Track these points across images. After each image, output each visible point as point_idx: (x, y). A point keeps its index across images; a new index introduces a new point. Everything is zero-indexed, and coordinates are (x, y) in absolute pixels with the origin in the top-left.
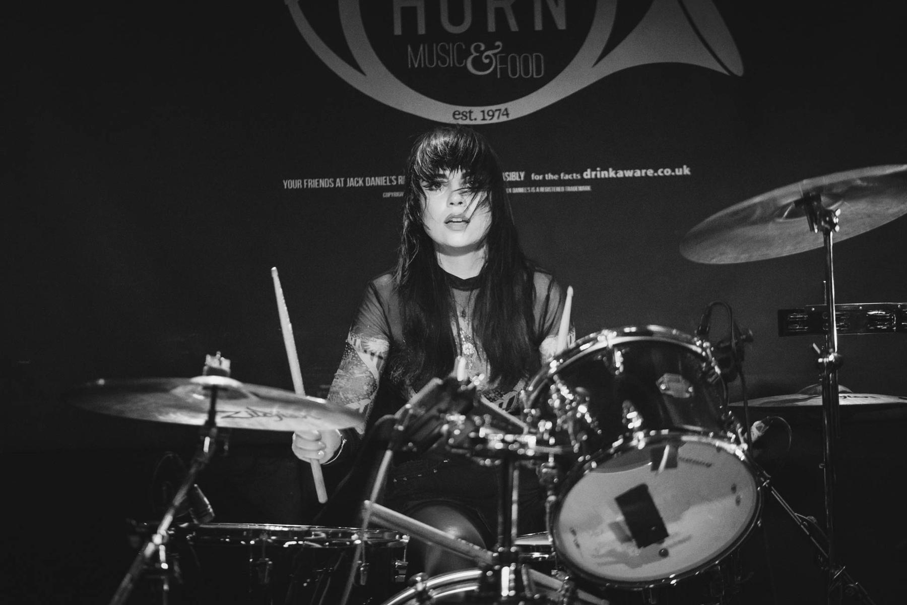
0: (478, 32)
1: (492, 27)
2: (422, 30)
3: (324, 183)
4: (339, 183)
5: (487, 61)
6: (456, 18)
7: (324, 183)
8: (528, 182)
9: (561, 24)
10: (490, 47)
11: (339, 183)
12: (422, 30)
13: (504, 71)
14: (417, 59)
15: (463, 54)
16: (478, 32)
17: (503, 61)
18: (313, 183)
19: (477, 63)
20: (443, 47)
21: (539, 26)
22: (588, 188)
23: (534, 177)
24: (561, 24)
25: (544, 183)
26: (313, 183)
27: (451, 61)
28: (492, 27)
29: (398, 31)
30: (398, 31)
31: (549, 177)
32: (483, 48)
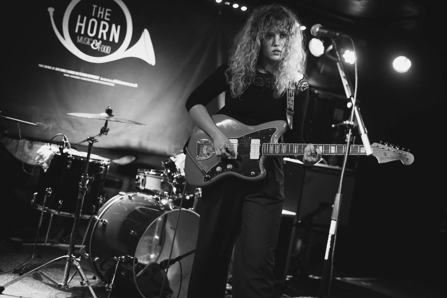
0: (96, 37)
1: (100, 37)
2: (82, 32)
3: (49, 67)
4: (53, 68)
5: (96, 45)
6: (92, 32)
7: (49, 67)
8: (99, 80)
9: (117, 41)
10: (98, 42)
11: (53, 68)
12: (82, 32)
13: (100, 49)
14: (80, 40)
15: (91, 42)
16: (96, 37)
17: (101, 46)
18: (46, 67)
19: (94, 45)
20: (87, 39)
21: (111, 40)
22: (113, 85)
23: (102, 79)
24: (117, 41)
25: (103, 81)
26: (46, 67)
27: (88, 43)
28: (100, 37)
29: (77, 31)
30: (77, 31)
31: (105, 79)
32: (96, 41)
